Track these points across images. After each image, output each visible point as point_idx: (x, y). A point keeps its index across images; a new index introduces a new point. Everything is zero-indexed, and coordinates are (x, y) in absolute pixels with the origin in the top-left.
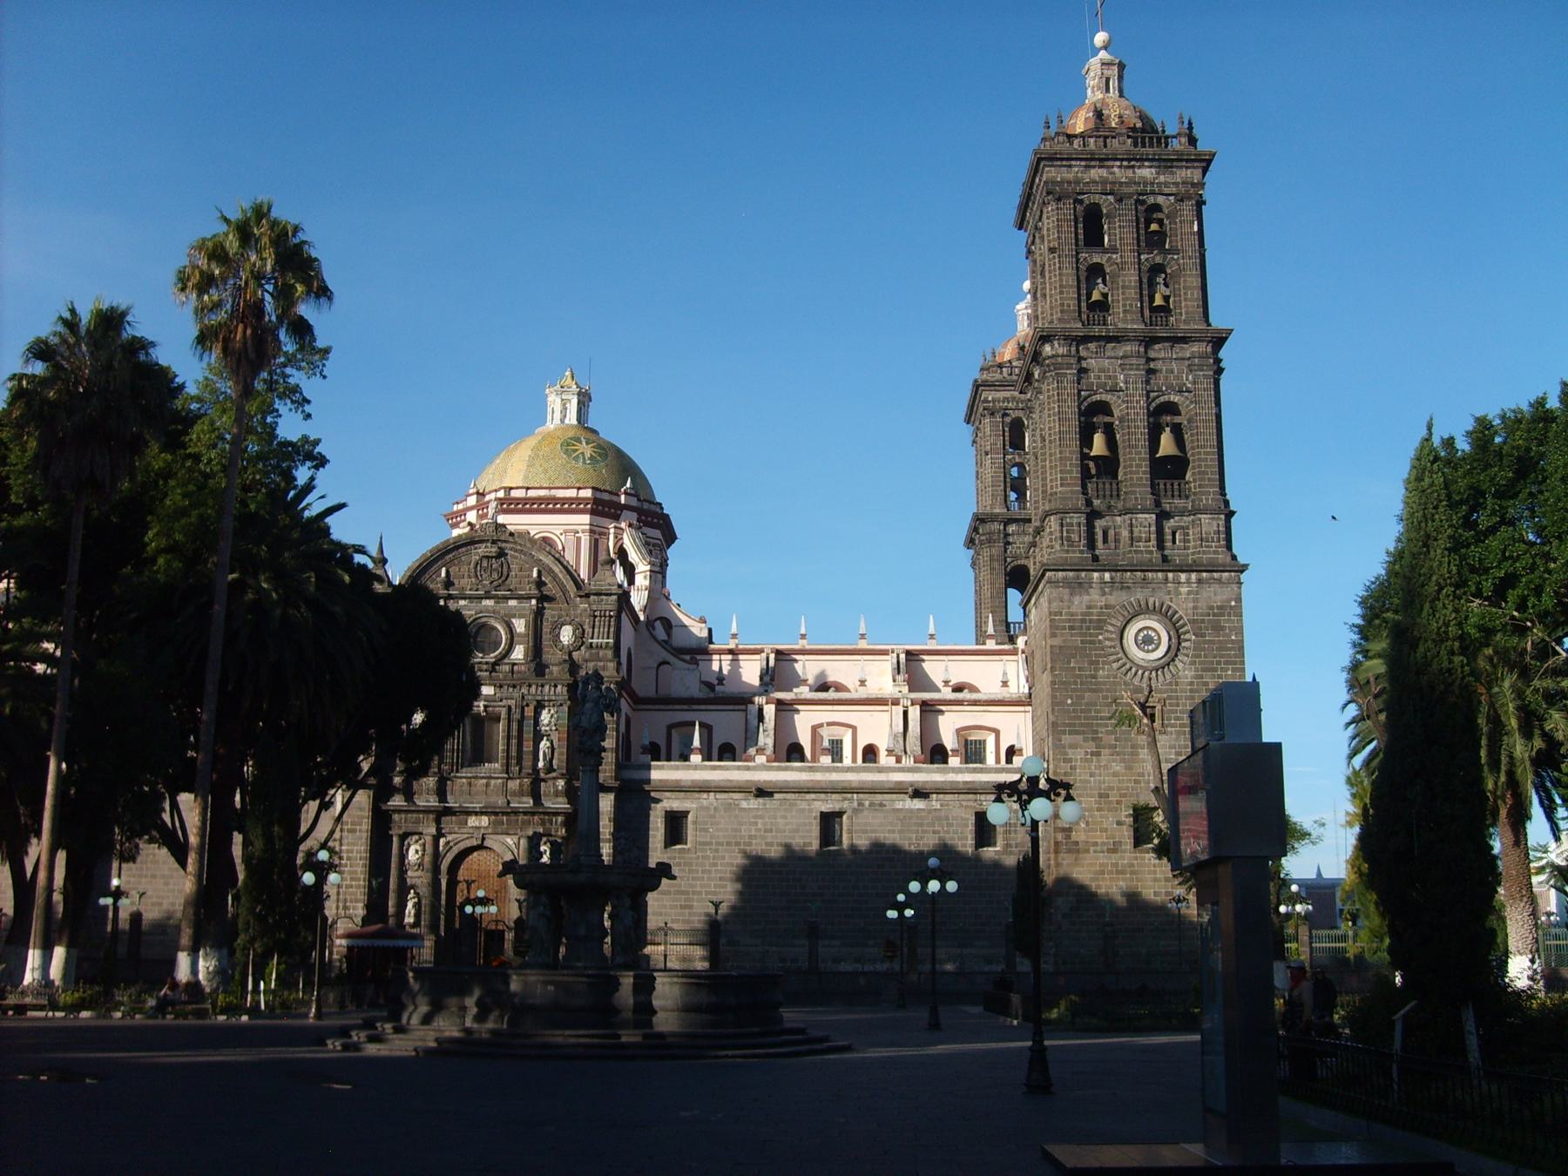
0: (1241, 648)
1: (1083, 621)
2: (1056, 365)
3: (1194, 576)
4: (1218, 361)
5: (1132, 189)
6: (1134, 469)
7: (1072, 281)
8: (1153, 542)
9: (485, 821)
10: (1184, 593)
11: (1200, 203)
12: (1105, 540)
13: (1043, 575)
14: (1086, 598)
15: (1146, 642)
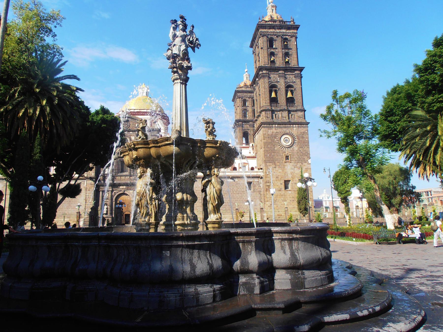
0: (308, 142)
1: (271, 136)
2: (263, 76)
3: (297, 126)
4: (301, 75)
5: (280, 34)
6: (282, 100)
7: (267, 55)
8: (287, 117)
9: (125, 187)
10: (295, 130)
11: (296, 38)
12: (276, 117)
13: (261, 126)
14: (272, 130)
15: (286, 141)
